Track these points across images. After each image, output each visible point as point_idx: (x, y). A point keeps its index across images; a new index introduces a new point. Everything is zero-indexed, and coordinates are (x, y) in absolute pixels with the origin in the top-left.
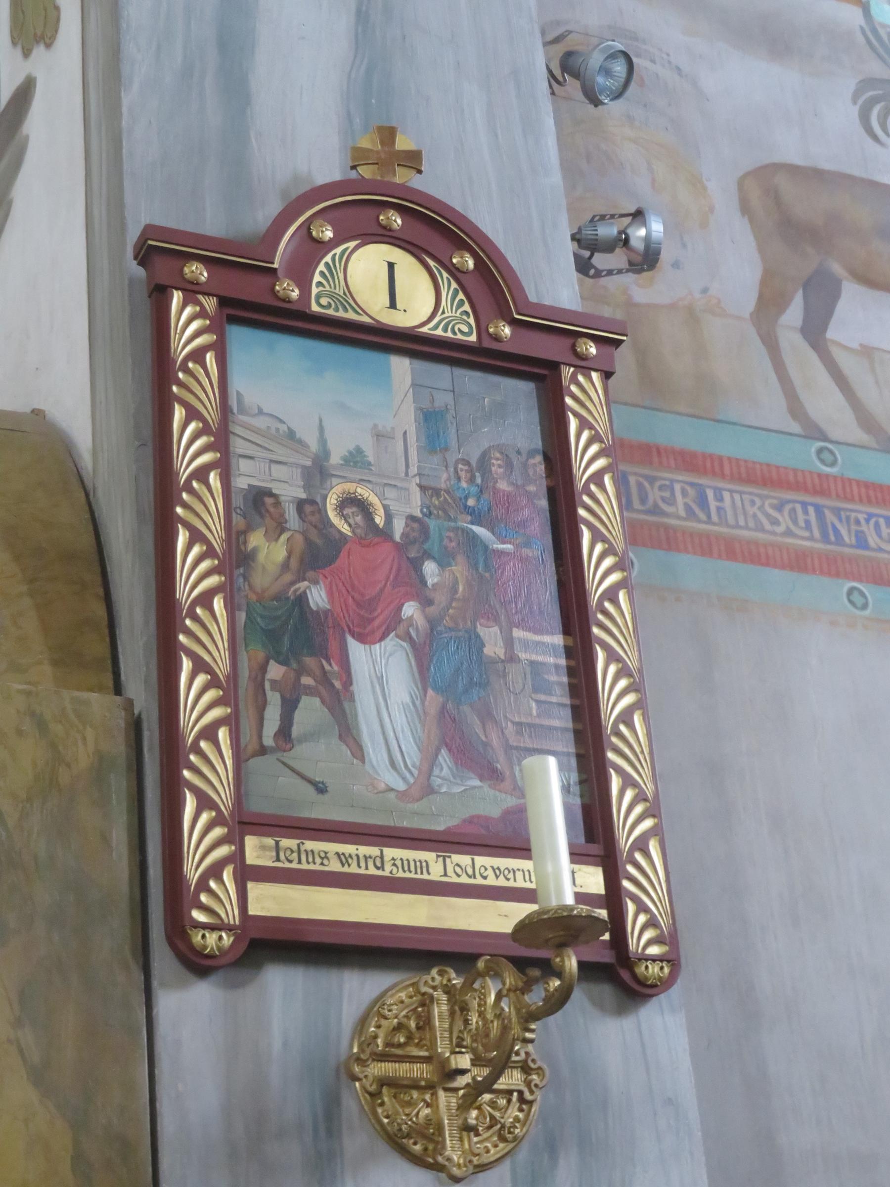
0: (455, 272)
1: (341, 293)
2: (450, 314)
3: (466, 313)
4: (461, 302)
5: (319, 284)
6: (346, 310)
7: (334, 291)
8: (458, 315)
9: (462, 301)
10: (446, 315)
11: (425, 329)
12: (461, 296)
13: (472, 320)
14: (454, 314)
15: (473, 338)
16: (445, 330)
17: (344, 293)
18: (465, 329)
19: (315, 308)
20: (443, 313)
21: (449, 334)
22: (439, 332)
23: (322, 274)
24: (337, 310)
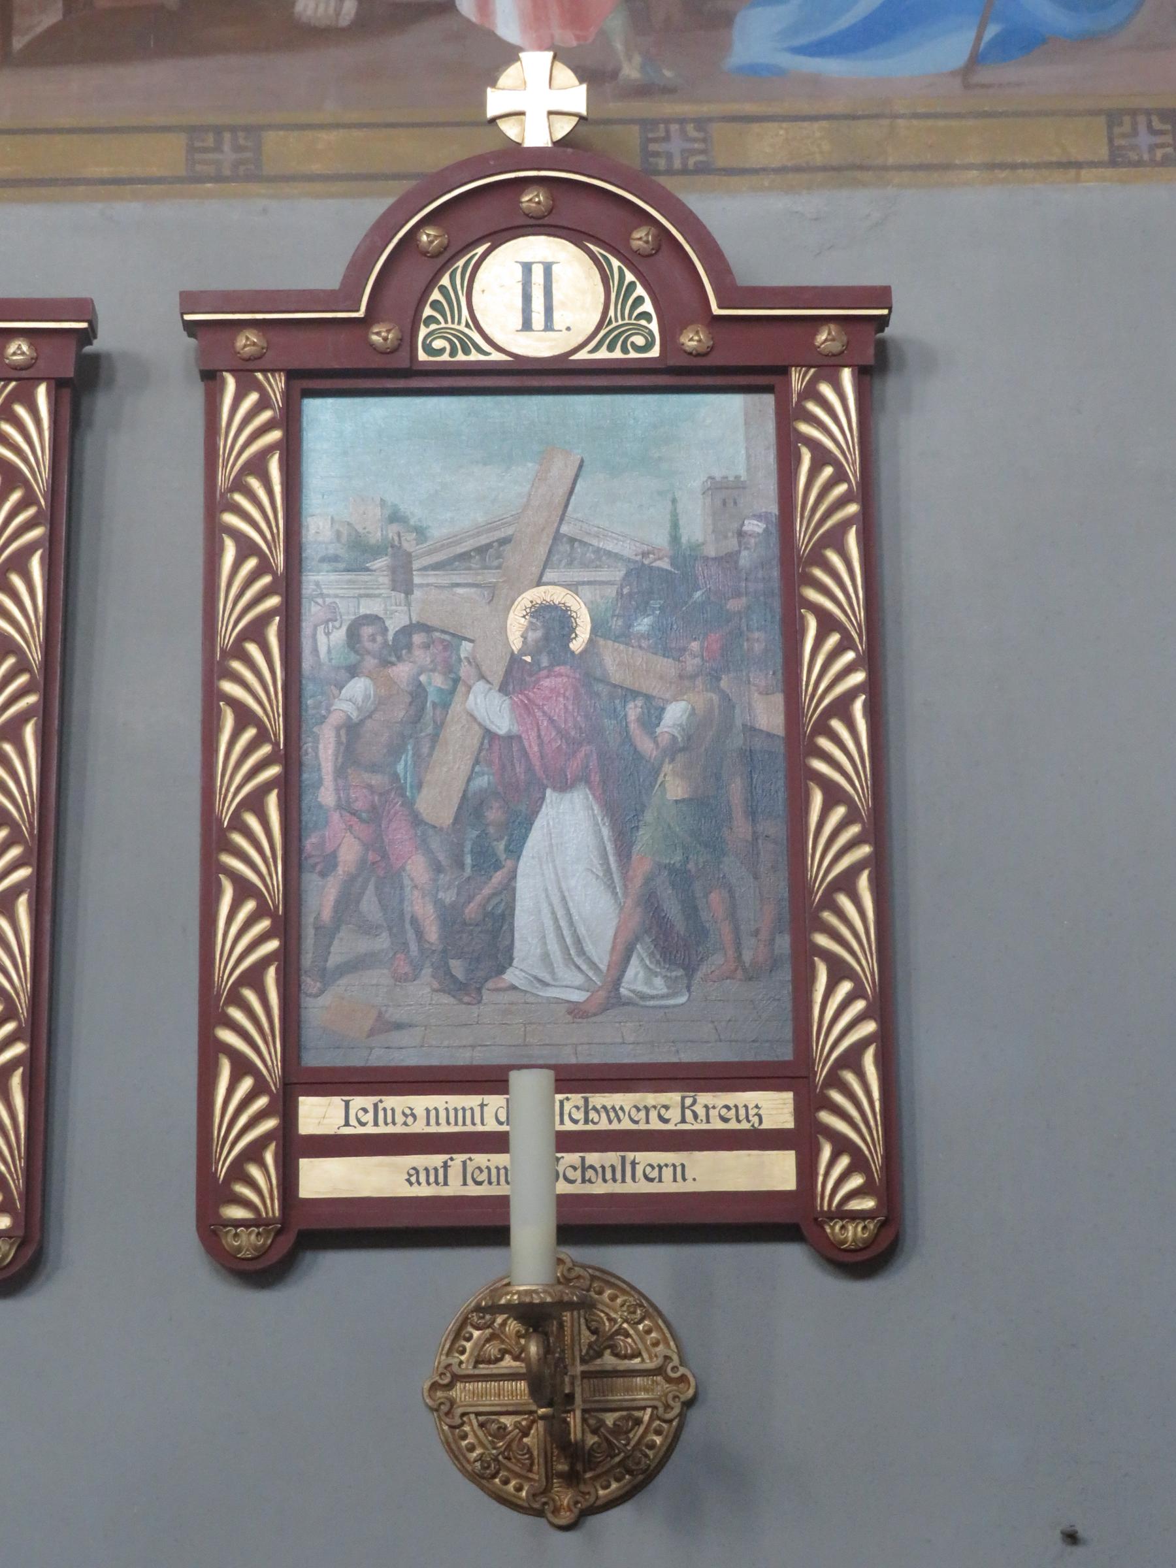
0: (630, 259)
1: (462, 328)
2: (620, 322)
3: (646, 316)
4: (639, 301)
5: (431, 320)
6: (466, 351)
7: (453, 326)
10: (614, 324)
11: (582, 355)
12: (640, 291)
13: (654, 326)
14: (627, 321)
17: (467, 325)
18: (640, 341)
20: (610, 322)
21: (617, 354)
22: (603, 354)
23: (436, 305)
24: (453, 353)
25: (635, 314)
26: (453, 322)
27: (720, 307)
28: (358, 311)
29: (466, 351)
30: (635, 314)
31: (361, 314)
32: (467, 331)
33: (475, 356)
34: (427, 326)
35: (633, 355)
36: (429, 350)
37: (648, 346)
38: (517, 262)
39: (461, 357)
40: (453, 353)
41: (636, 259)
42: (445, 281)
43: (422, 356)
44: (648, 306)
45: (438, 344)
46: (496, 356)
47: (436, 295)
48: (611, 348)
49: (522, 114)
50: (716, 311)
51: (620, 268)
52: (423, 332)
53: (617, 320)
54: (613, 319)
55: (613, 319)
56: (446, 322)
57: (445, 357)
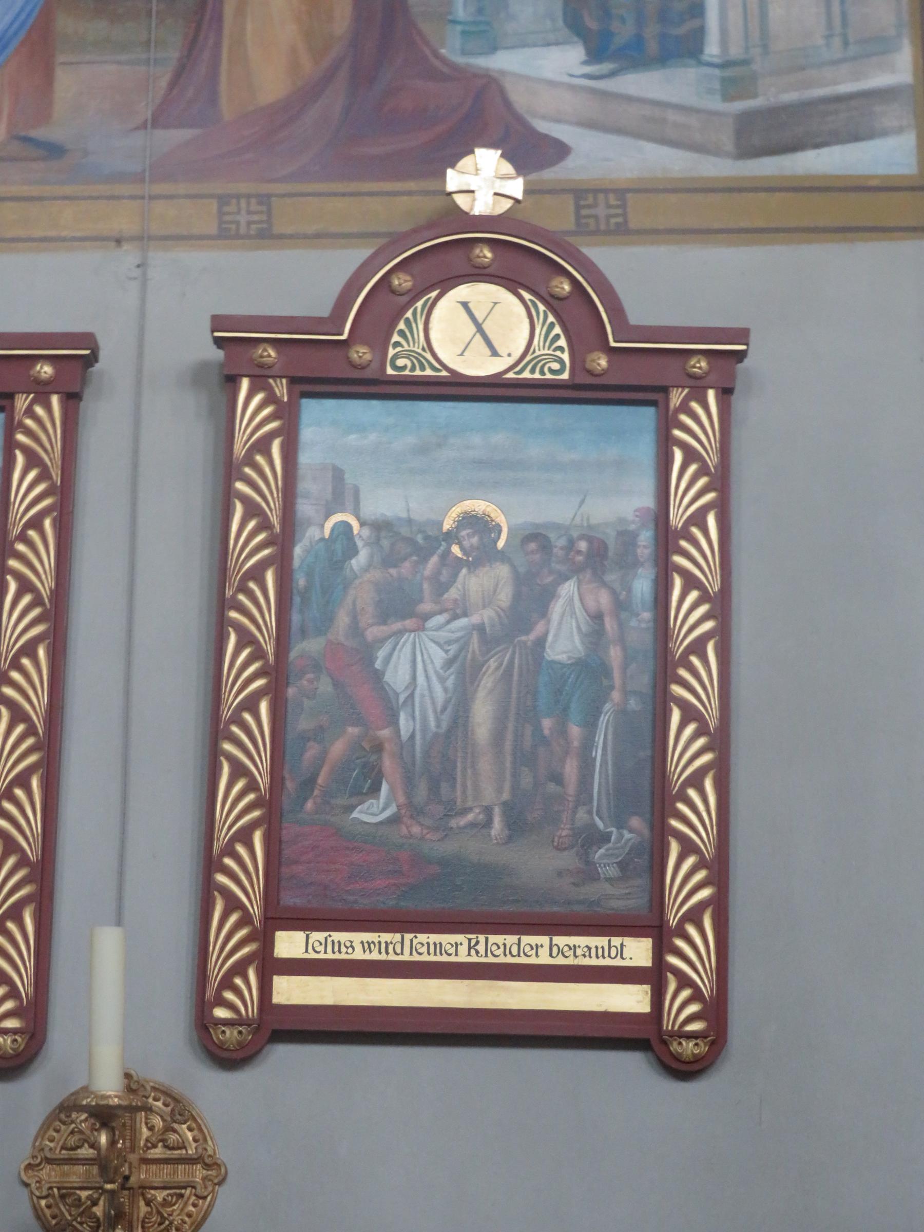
1: (420, 351)
2: (542, 352)
3: (561, 349)
4: (557, 337)
5: (397, 344)
6: (423, 368)
8: (550, 352)
9: (557, 337)
10: (536, 355)
11: (511, 375)
12: (557, 330)
13: (566, 357)
14: (547, 352)
15: (565, 376)
16: (533, 371)
17: (423, 349)
18: (556, 366)
19: (390, 371)
20: (534, 352)
21: (537, 376)
22: (526, 375)
23: (402, 333)
24: (413, 369)
25: (553, 347)
26: (414, 346)
27: (615, 341)
28: (341, 334)
29: (423, 368)
30: (553, 347)
31: (344, 337)
32: (423, 353)
33: (429, 372)
34: (394, 348)
35: (549, 376)
36: (395, 367)
37: (561, 371)
38: (458, 302)
39: (418, 372)
40: (413, 369)
41: (555, 303)
42: (409, 314)
43: (390, 371)
44: (562, 342)
45: (400, 362)
46: (444, 373)
47: (402, 325)
48: (533, 371)
49: (473, 192)
50: (613, 344)
51: (545, 312)
52: (391, 352)
53: (539, 350)
54: (537, 348)
55: (537, 348)
56: (409, 346)
57: (407, 372)
